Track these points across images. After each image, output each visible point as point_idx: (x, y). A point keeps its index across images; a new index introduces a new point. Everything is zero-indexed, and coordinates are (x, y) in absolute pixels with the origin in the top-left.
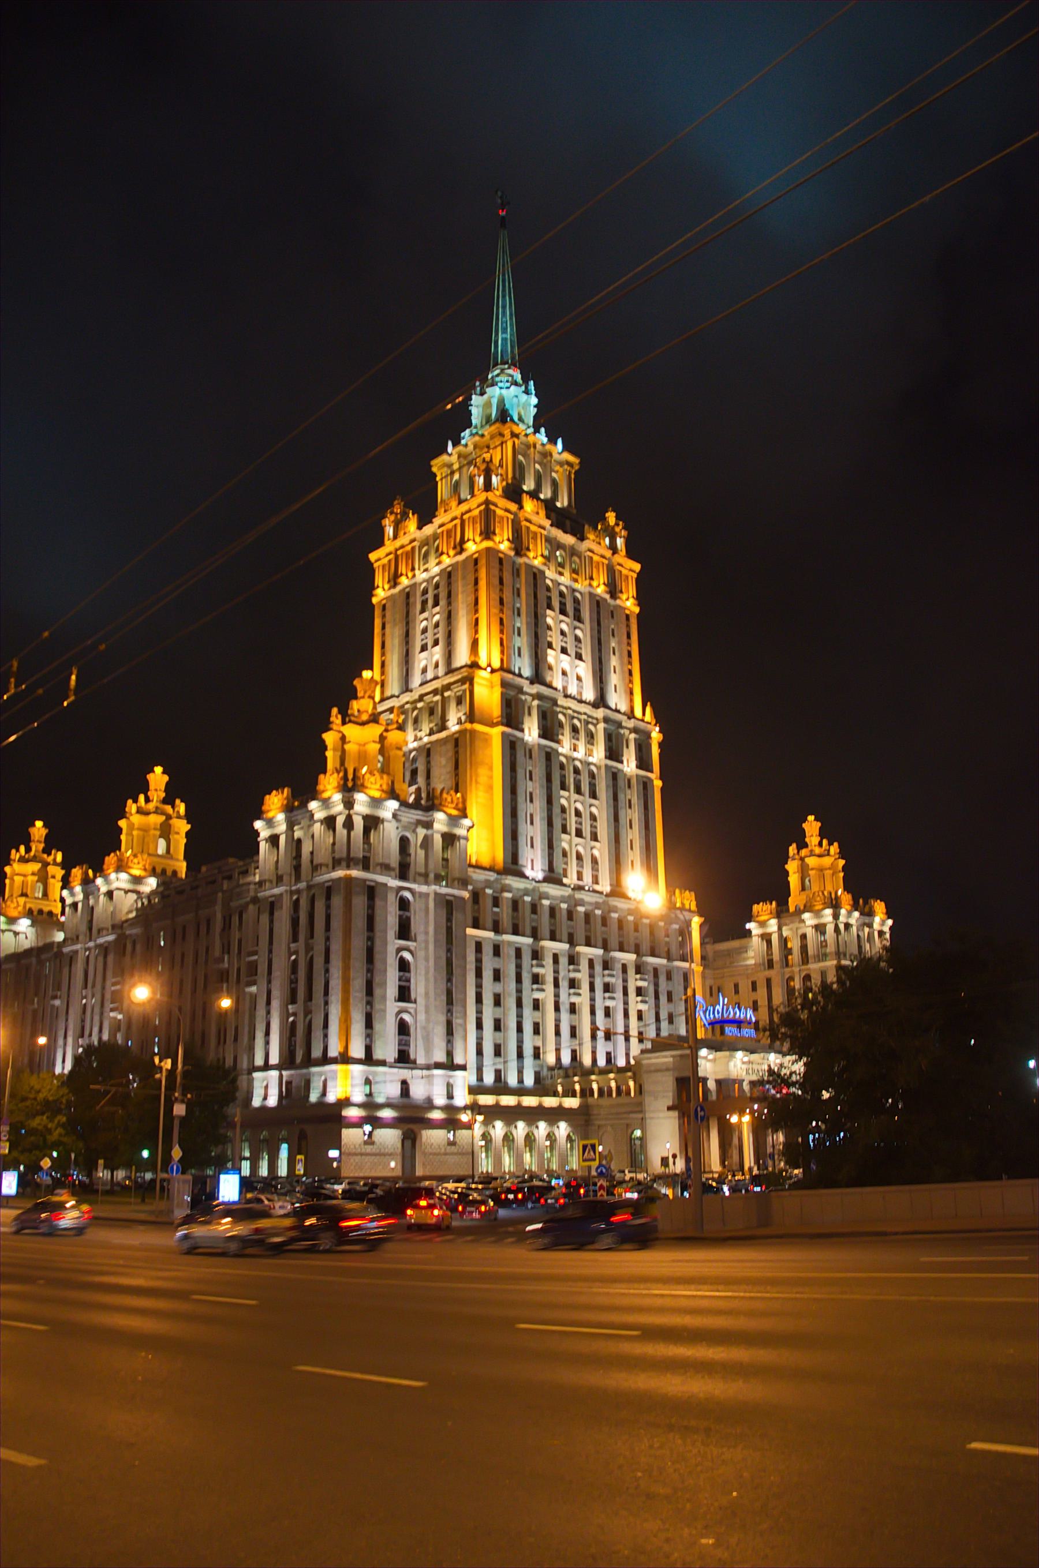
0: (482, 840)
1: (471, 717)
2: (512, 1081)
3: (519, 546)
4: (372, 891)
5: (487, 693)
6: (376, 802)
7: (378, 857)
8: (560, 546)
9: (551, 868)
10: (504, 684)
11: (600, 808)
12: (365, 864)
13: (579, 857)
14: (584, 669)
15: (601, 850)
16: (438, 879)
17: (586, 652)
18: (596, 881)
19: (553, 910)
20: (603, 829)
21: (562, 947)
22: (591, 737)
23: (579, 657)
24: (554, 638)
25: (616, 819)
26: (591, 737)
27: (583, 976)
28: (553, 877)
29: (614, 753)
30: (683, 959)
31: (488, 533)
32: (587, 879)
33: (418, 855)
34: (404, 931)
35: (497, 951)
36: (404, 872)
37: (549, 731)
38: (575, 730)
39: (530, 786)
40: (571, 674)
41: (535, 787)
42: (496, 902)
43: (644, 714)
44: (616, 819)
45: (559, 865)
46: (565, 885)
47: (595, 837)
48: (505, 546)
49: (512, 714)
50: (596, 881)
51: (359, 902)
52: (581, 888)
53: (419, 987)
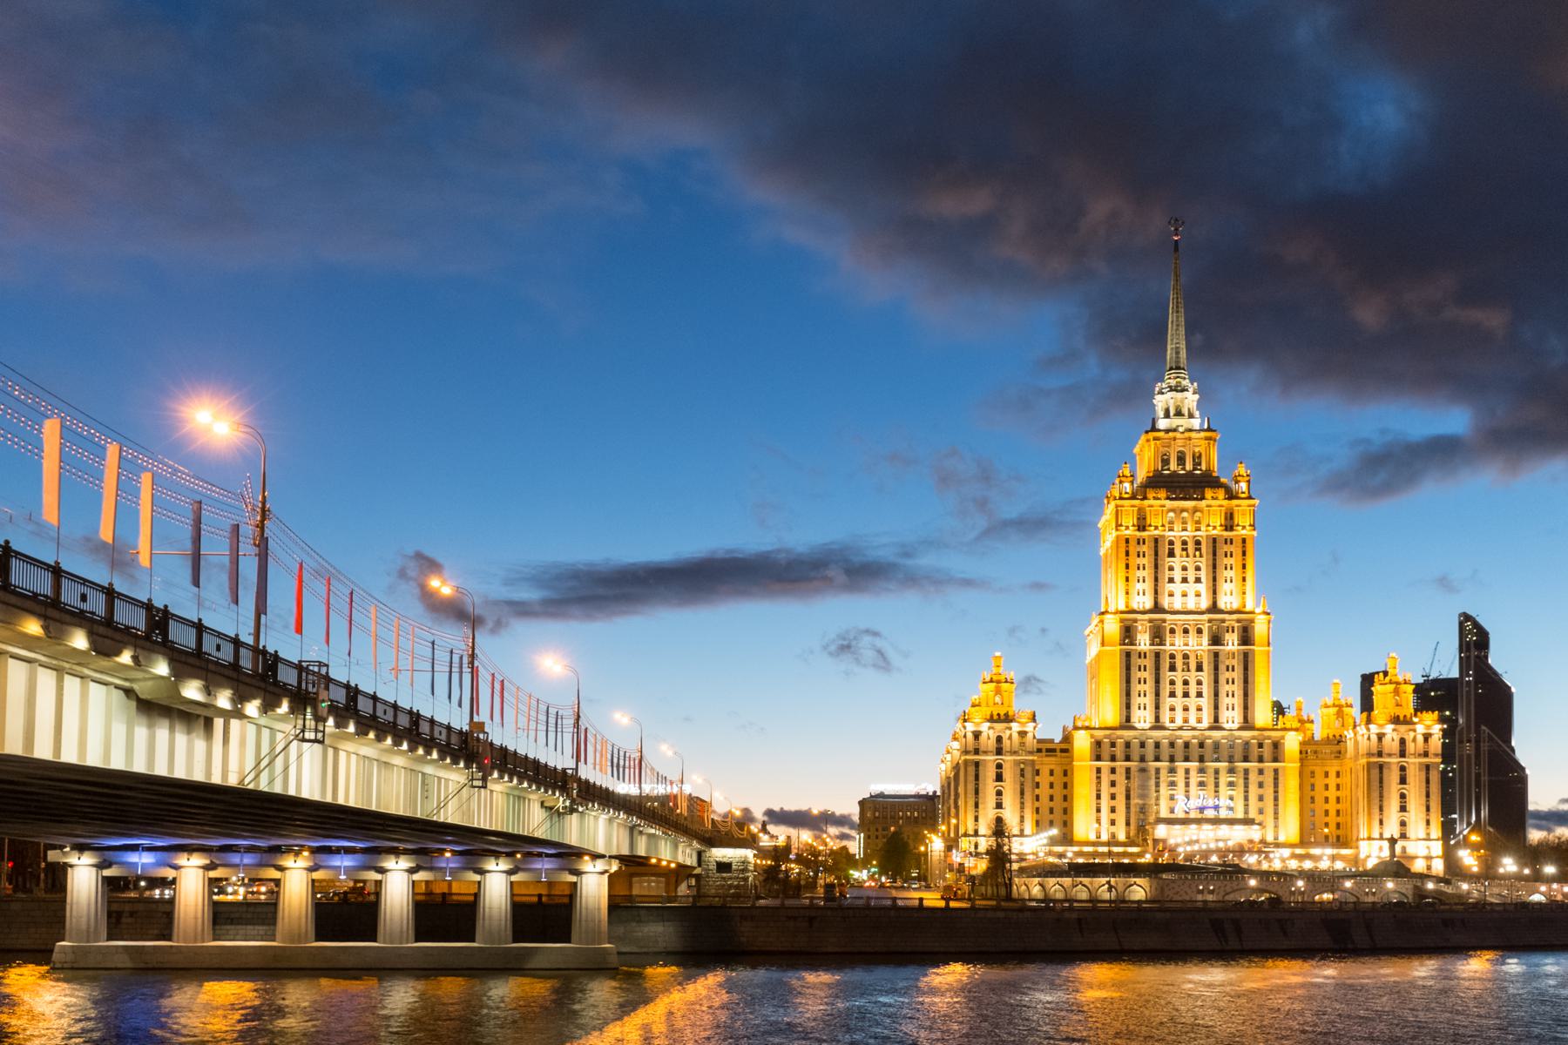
0: (1109, 713)
1: (1103, 644)
2: (1122, 837)
3: (1142, 527)
4: (977, 764)
5: (1113, 626)
6: (978, 724)
7: (982, 748)
8: (1183, 510)
9: (1157, 719)
10: (1122, 621)
11: (1206, 676)
12: (977, 752)
13: (1186, 709)
14: (1202, 588)
15: (1205, 702)
16: (1015, 753)
17: (1203, 575)
18: (1199, 721)
19: (1157, 745)
20: (1206, 689)
21: (1164, 765)
22: (1200, 631)
23: (1198, 580)
24: (1178, 574)
25: (1216, 681)
26: (1200, 631)
27: (1180, 778)
28: (1158, 725)
29: (1216, 640)
30: (1276, 760)
31: (1118, 526)
32: (1193, 722)
33: (1006, 743)
34: (999, 778)
35: (1113, 771)
36: (999, 751)
37: (1158, 635)
38: (1186, 631)
39: (1143, 675)
40: (1186, 595)
41: (1148, 675)
42: (1113, 745)
43: (1258, 604)
44: (1216, 681)
45: (1165, 717)
46: (1163, 728)
47: (1199, 695)
48: (1131, 532)
49: (1128, 633)
50: (1199, 721)
51: (971, 770)
52: (1180, 728)
53: (1009, 800)
